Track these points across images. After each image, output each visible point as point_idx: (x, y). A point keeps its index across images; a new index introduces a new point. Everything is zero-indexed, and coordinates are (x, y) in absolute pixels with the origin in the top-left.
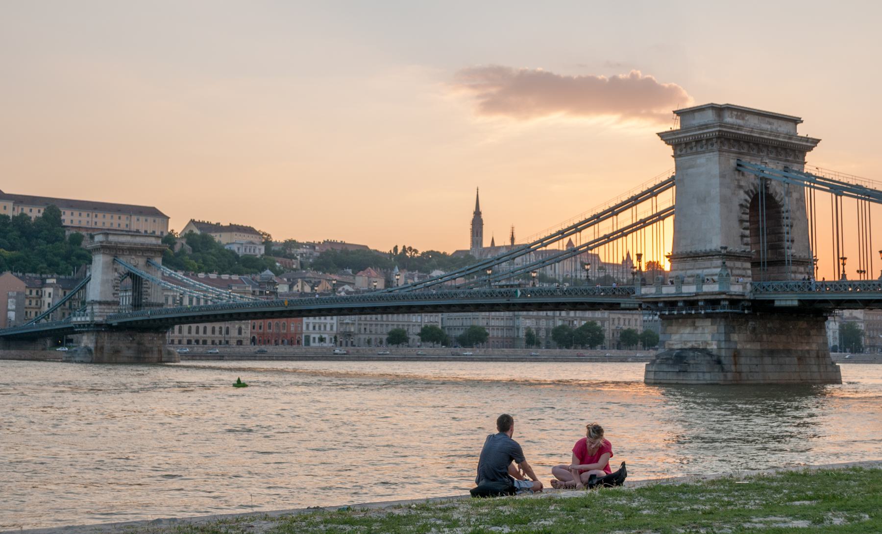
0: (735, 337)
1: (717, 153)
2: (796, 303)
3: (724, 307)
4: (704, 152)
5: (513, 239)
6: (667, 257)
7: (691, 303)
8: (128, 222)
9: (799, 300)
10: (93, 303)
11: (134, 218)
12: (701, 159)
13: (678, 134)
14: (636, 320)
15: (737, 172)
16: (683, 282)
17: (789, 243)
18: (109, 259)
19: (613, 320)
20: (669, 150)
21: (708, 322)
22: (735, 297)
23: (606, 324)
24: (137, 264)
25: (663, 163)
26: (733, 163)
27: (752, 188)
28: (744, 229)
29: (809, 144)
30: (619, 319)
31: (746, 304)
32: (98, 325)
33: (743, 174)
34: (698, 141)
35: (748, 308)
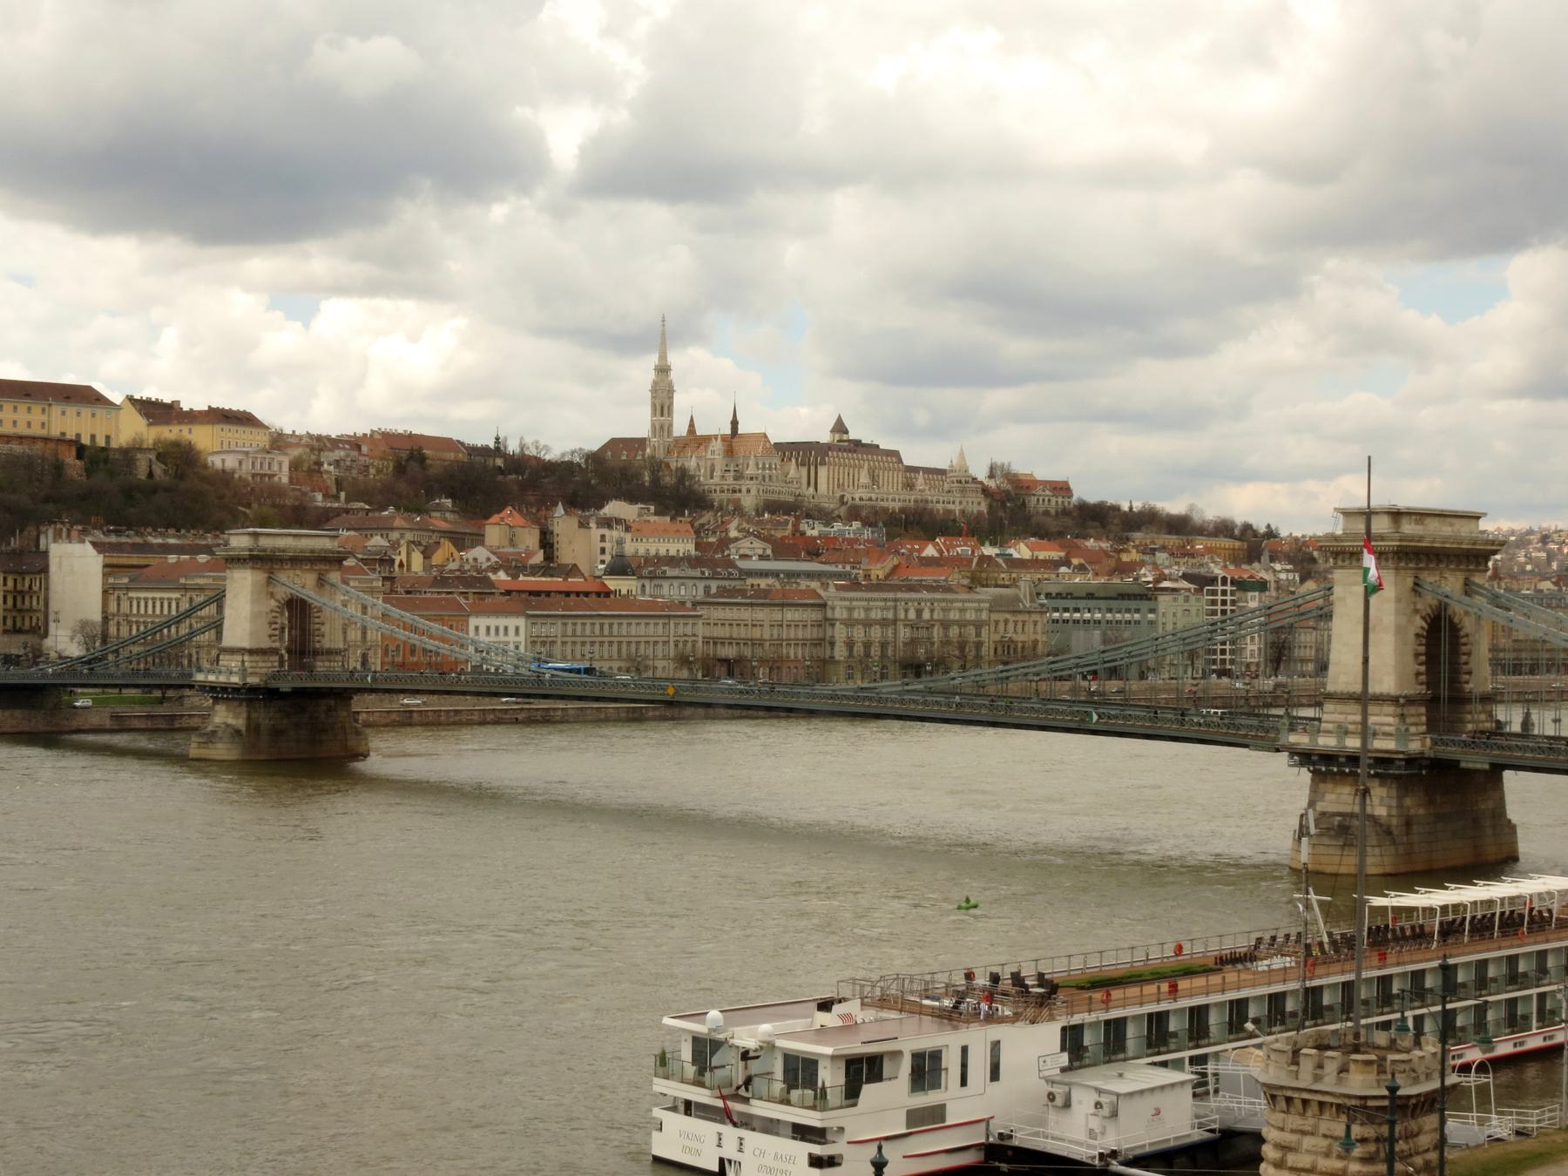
0: (1408, 801)
2: (1487, 767)
3: (1399, 768)
5: (735, 423)
8: (44, 418)
10: (232, 651)
11: (56, 410)
14: (1035, 623)
16: (1347, 733)
18: (261, 576)
19: (997, 622)
23: (984, 631)
24: (301, 583)
26: (1410, 581)
30: (1006, 621)
31: (1425, 763)
32: (253, 690)
35: (1426, 767)
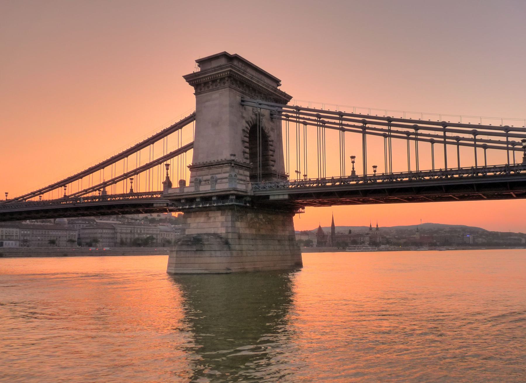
0: (238, 224)
1: (228, 89)
2: (286, 197)
3: (232, 200)
4: (218, 89)
6: (188, 167)
7: (206, 199)
9: (289, 195)
12: (215, 95)
13: (199, 75)
15: (241, 106)
17: (273, 163)
20: (192, 89)
21: (219, 213)
22: (241, 193)
25: (187, 101)
26: (239, 98)
27: (251, 120)
28: (246, 147)
29: (286, 98)
33: (245, 109)
34: (214, 81)
35: (249, 202)
